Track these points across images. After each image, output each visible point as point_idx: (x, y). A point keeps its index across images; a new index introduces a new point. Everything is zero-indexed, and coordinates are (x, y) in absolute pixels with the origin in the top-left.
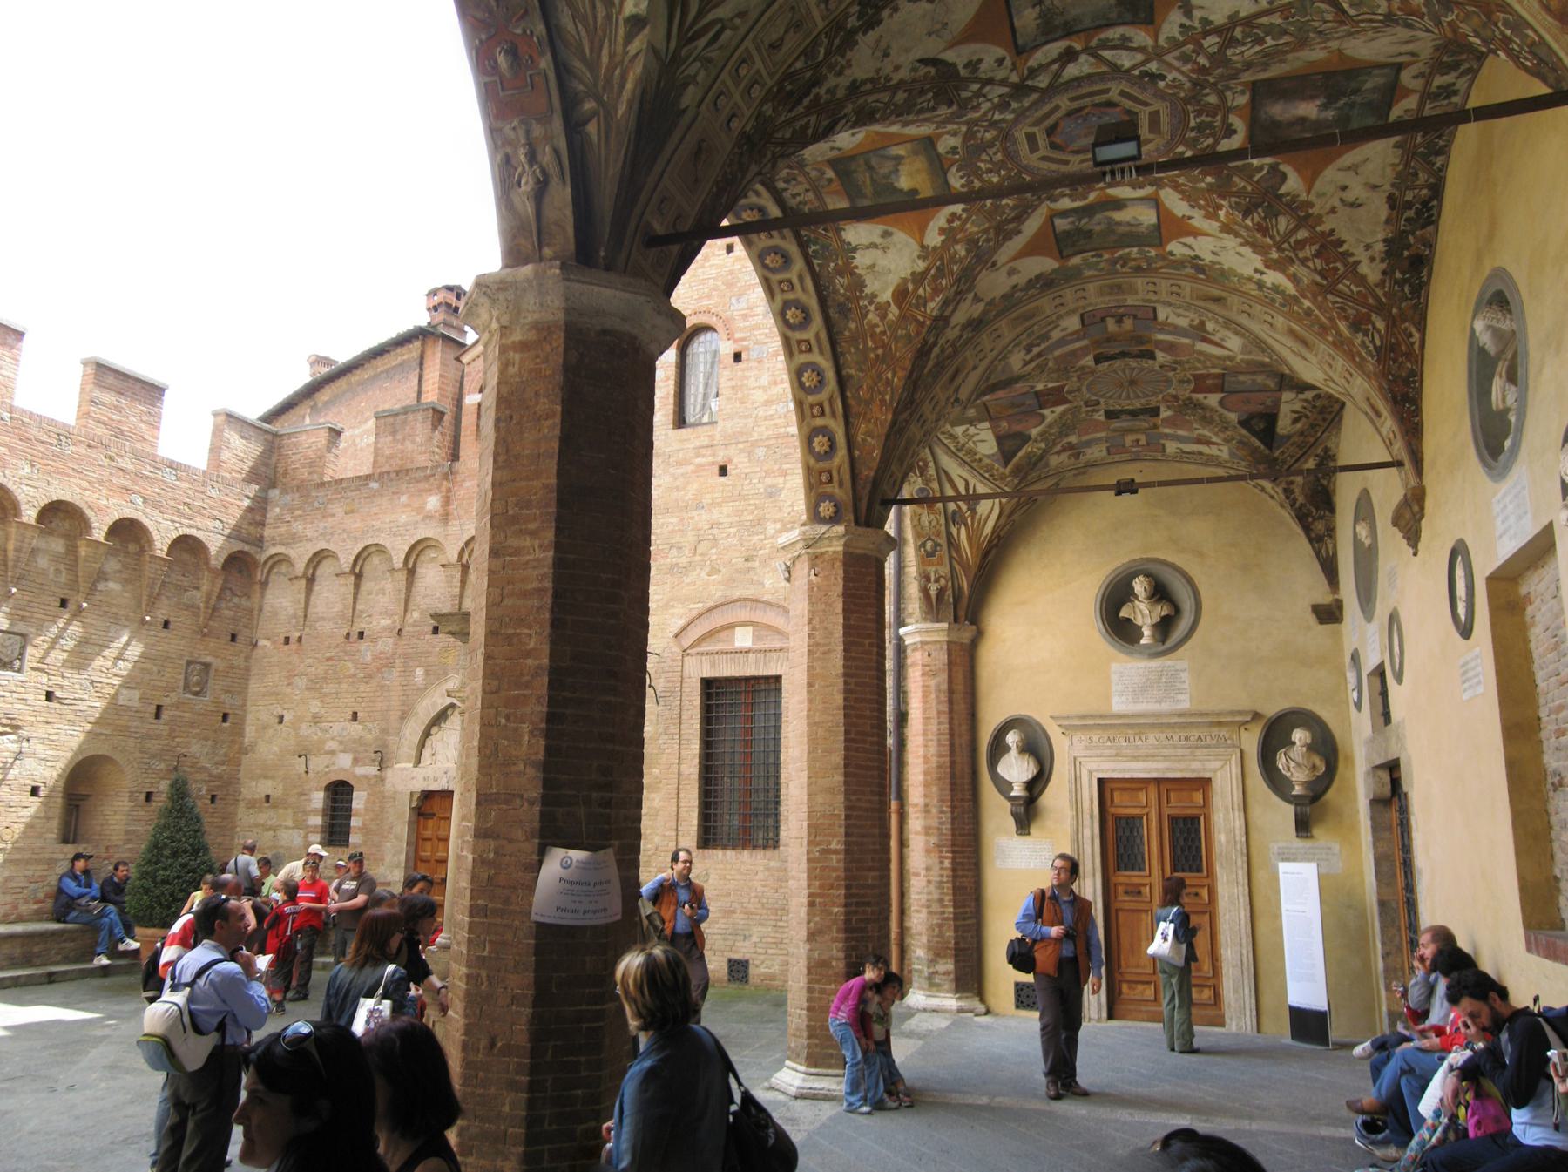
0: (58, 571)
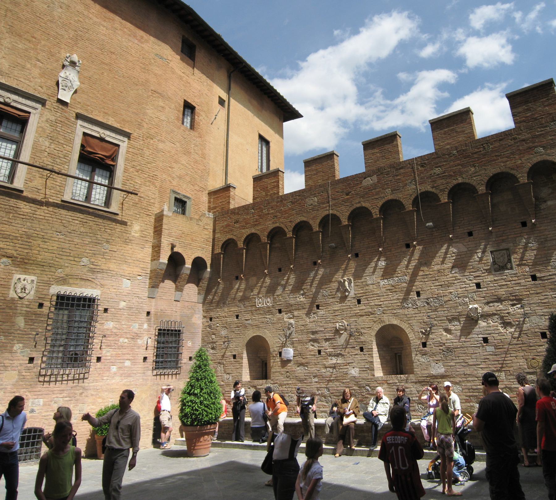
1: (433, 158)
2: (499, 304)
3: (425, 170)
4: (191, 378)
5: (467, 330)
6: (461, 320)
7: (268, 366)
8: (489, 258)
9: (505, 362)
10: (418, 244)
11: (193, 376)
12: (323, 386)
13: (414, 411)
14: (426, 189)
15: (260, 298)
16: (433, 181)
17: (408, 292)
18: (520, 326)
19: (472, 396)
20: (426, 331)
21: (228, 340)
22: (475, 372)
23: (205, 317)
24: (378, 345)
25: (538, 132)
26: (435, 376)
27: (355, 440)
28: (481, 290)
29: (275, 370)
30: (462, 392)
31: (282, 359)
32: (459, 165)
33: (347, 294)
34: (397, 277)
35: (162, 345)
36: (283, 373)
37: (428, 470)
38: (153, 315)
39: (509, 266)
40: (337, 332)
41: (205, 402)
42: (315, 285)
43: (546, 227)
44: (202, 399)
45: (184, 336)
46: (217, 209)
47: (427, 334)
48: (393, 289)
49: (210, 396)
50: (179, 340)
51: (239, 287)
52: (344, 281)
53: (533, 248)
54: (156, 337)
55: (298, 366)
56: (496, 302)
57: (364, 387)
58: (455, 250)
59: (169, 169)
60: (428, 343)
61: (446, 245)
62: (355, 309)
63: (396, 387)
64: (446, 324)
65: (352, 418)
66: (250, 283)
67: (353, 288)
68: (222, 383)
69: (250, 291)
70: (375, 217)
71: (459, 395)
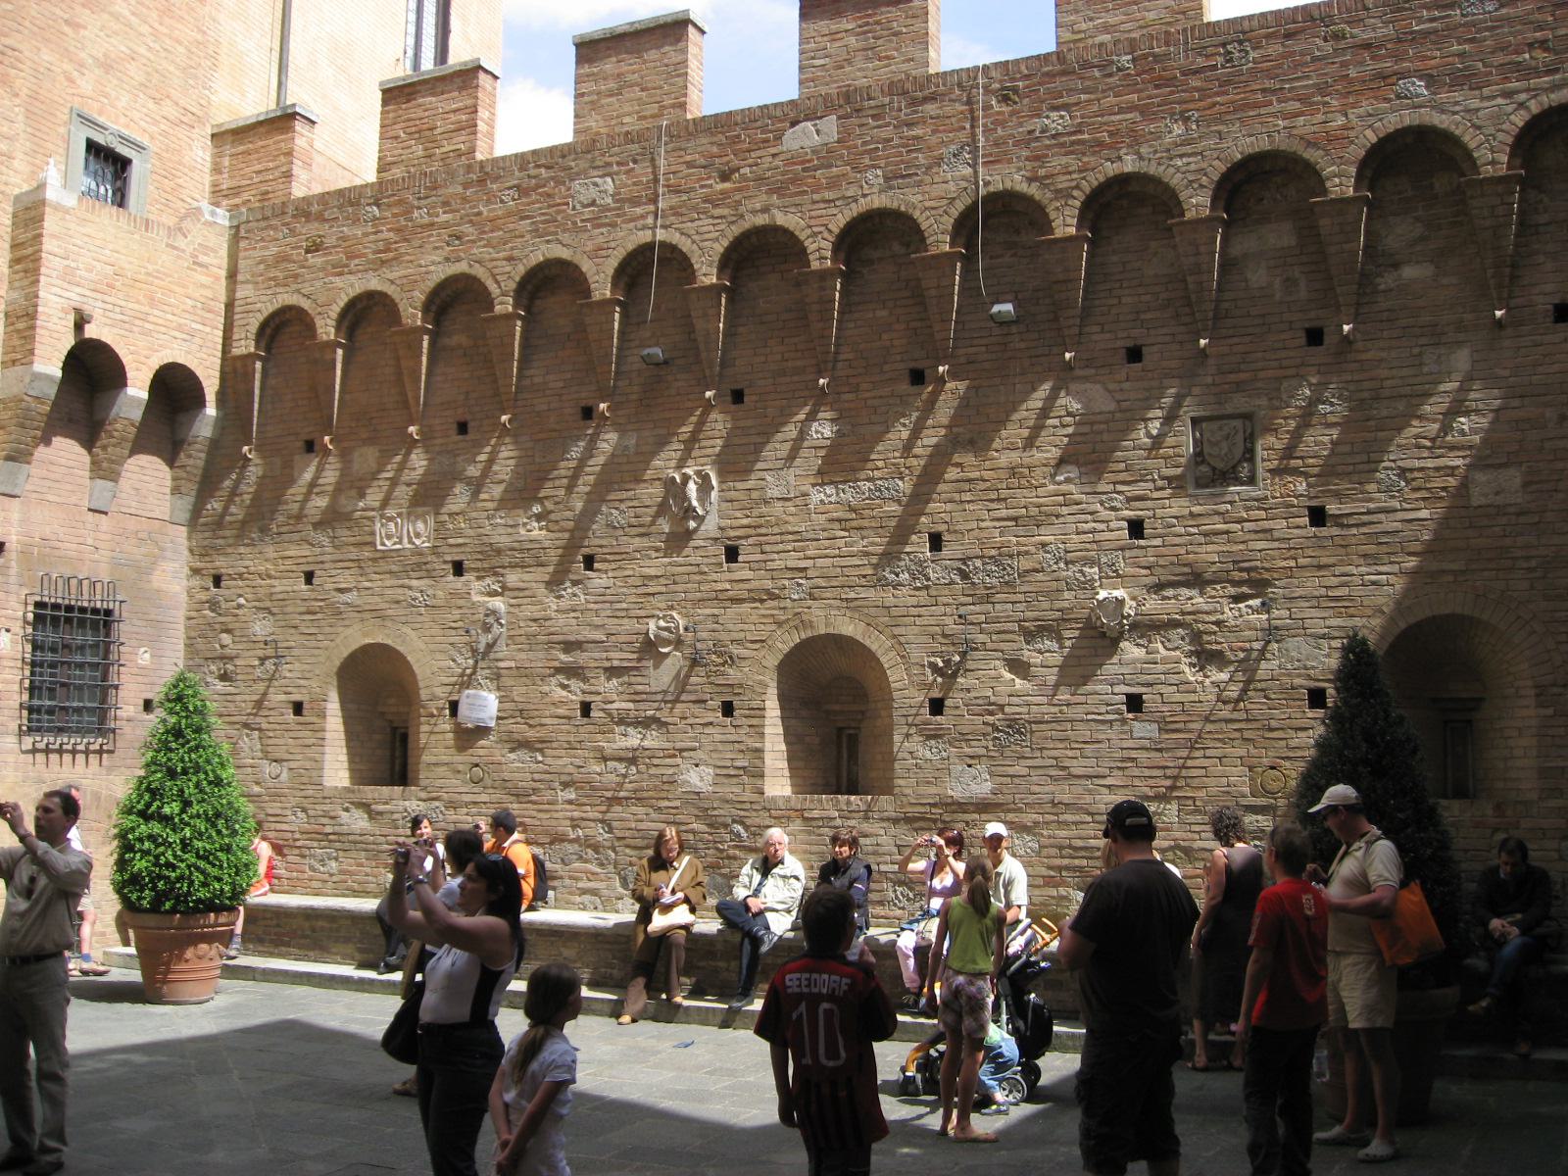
0: (1290, 283)
1: (1047, 74)
2: (1194, 592)
3: (1013, 113)
4: (148, 765)
5: (1078, 670)
6: (1067, 634)
7: (410, 745)
8: (1184, 441)
9: (1184, 773)
10: (954, 375)
11: (154, 762)
12: (591, 815)
13: (881, 903)
14: (1008, 185)
15: (391, 519)
16: (1037, 158)
17: (901, 534)
18: (1248, 667)
19: (1067, 868)
20: (947, 662)
21: (274, 654)
22: (1088, 799)
23: (196, 571)
24: (783, 699)
25: (1420, 20)
26: (960, 804)
27: (684, 980)
28: (1142, 542)
29: (433, 759)
30: (1039, 854)
31: (458, 725)
32: (1132, 108)
33: (692, 524)
34: (868, 480)
35: (49, 656)
36: (460, 767)
37: (904, 1070)
38: (14, 556)
39: (1244, 472)
40: (649, 648)
41: (198, 844)
42: (582, 488)
43: (1384, 355)
44: (187, 832)
45: (124, 630)
46: (245, 196)
47: (949, 673)
48: (851, 520)
49: (214, 825)
50: (108, 645)
51: (316, 479)
52: (686, 478)
53: (1331, 419)
54: (30, 630)
55: (512, 750)
56: (1187, 585)
57: (726, 826)
58: (1076, 406)
59: (66, 29)
60: (948, 702)
61: (1047, 386)
62: (715, 576)
63: (830, 832)
64: (1015, 646)
65: (681, 915)
66: (356, 466)
67: (714, 509)
68: (257, 789)
69: (353, 493)
70: (815, 265)
71: (1026, 865)
